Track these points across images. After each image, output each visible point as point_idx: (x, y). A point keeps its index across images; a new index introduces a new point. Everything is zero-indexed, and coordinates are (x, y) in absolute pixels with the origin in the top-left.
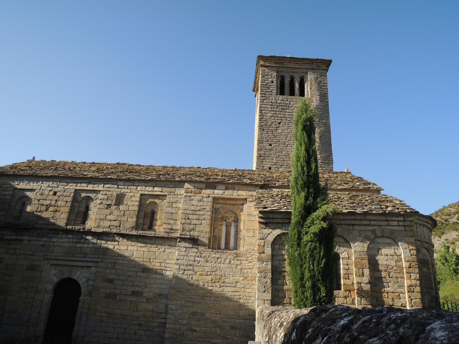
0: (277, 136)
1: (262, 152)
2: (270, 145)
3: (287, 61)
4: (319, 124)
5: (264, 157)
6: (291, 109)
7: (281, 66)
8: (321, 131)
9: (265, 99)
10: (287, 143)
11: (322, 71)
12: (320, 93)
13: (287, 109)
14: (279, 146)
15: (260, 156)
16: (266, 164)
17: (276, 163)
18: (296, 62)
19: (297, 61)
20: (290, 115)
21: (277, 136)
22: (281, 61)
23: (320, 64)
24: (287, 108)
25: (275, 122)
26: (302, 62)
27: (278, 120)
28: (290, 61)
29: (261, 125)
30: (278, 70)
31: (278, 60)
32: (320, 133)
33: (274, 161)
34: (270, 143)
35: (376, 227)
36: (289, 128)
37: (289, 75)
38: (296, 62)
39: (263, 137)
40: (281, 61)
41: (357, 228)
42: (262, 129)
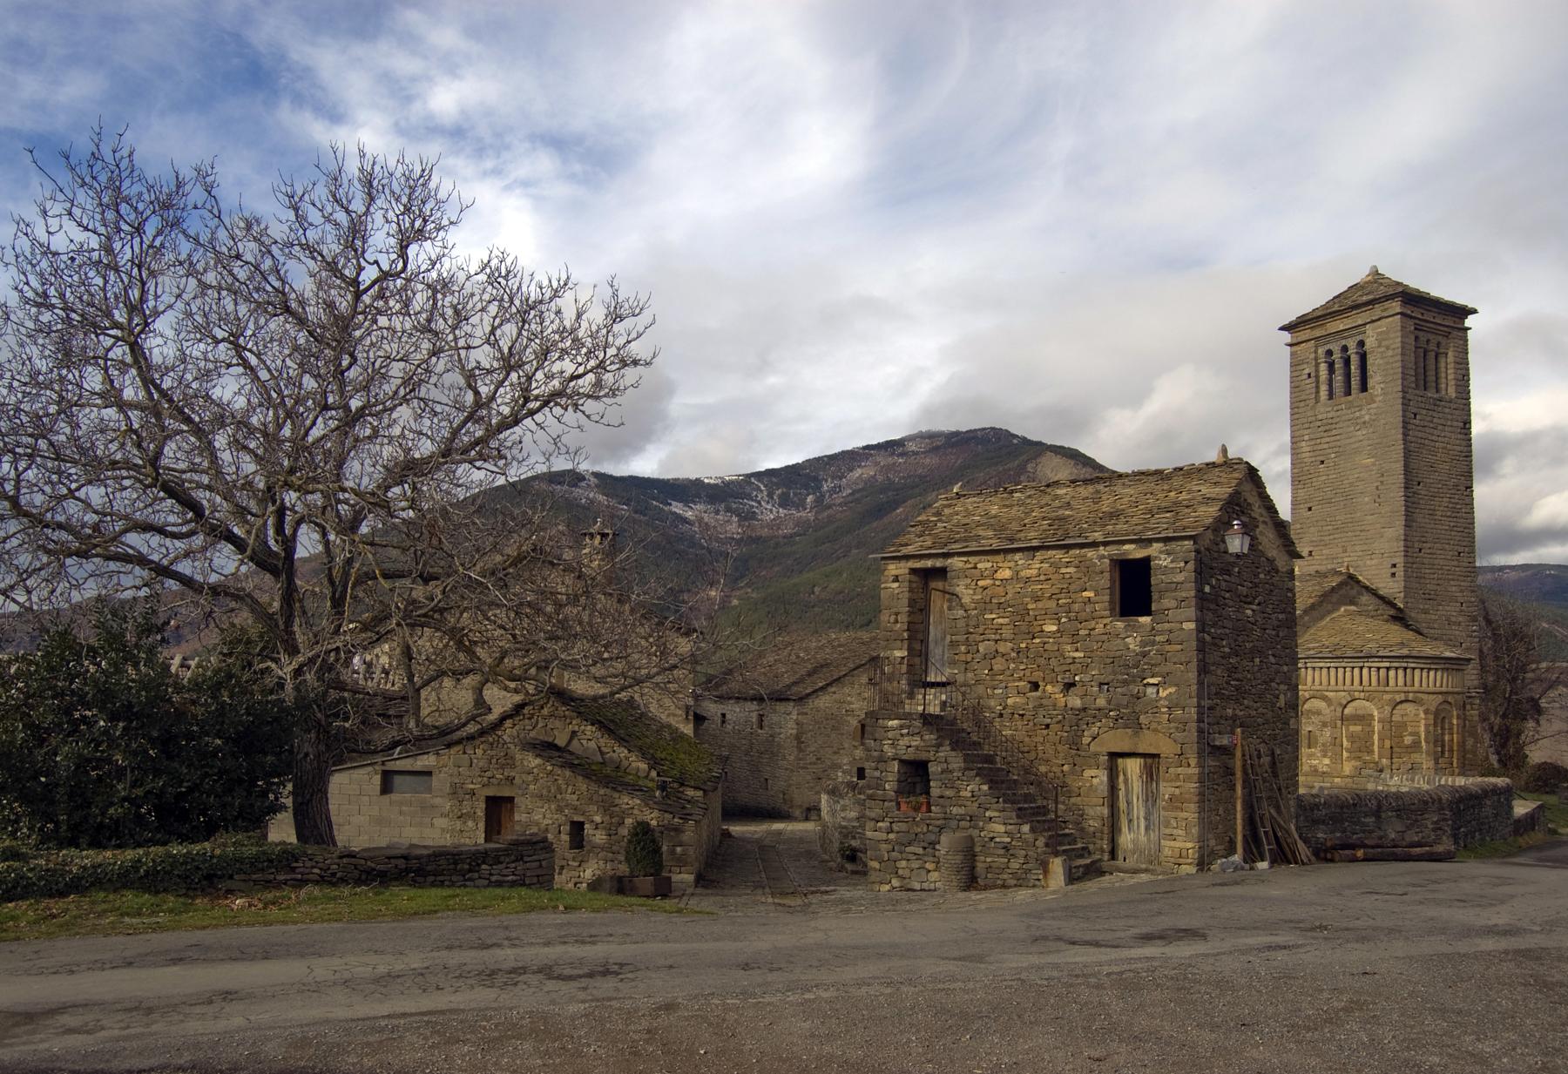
2: (1310, 509)
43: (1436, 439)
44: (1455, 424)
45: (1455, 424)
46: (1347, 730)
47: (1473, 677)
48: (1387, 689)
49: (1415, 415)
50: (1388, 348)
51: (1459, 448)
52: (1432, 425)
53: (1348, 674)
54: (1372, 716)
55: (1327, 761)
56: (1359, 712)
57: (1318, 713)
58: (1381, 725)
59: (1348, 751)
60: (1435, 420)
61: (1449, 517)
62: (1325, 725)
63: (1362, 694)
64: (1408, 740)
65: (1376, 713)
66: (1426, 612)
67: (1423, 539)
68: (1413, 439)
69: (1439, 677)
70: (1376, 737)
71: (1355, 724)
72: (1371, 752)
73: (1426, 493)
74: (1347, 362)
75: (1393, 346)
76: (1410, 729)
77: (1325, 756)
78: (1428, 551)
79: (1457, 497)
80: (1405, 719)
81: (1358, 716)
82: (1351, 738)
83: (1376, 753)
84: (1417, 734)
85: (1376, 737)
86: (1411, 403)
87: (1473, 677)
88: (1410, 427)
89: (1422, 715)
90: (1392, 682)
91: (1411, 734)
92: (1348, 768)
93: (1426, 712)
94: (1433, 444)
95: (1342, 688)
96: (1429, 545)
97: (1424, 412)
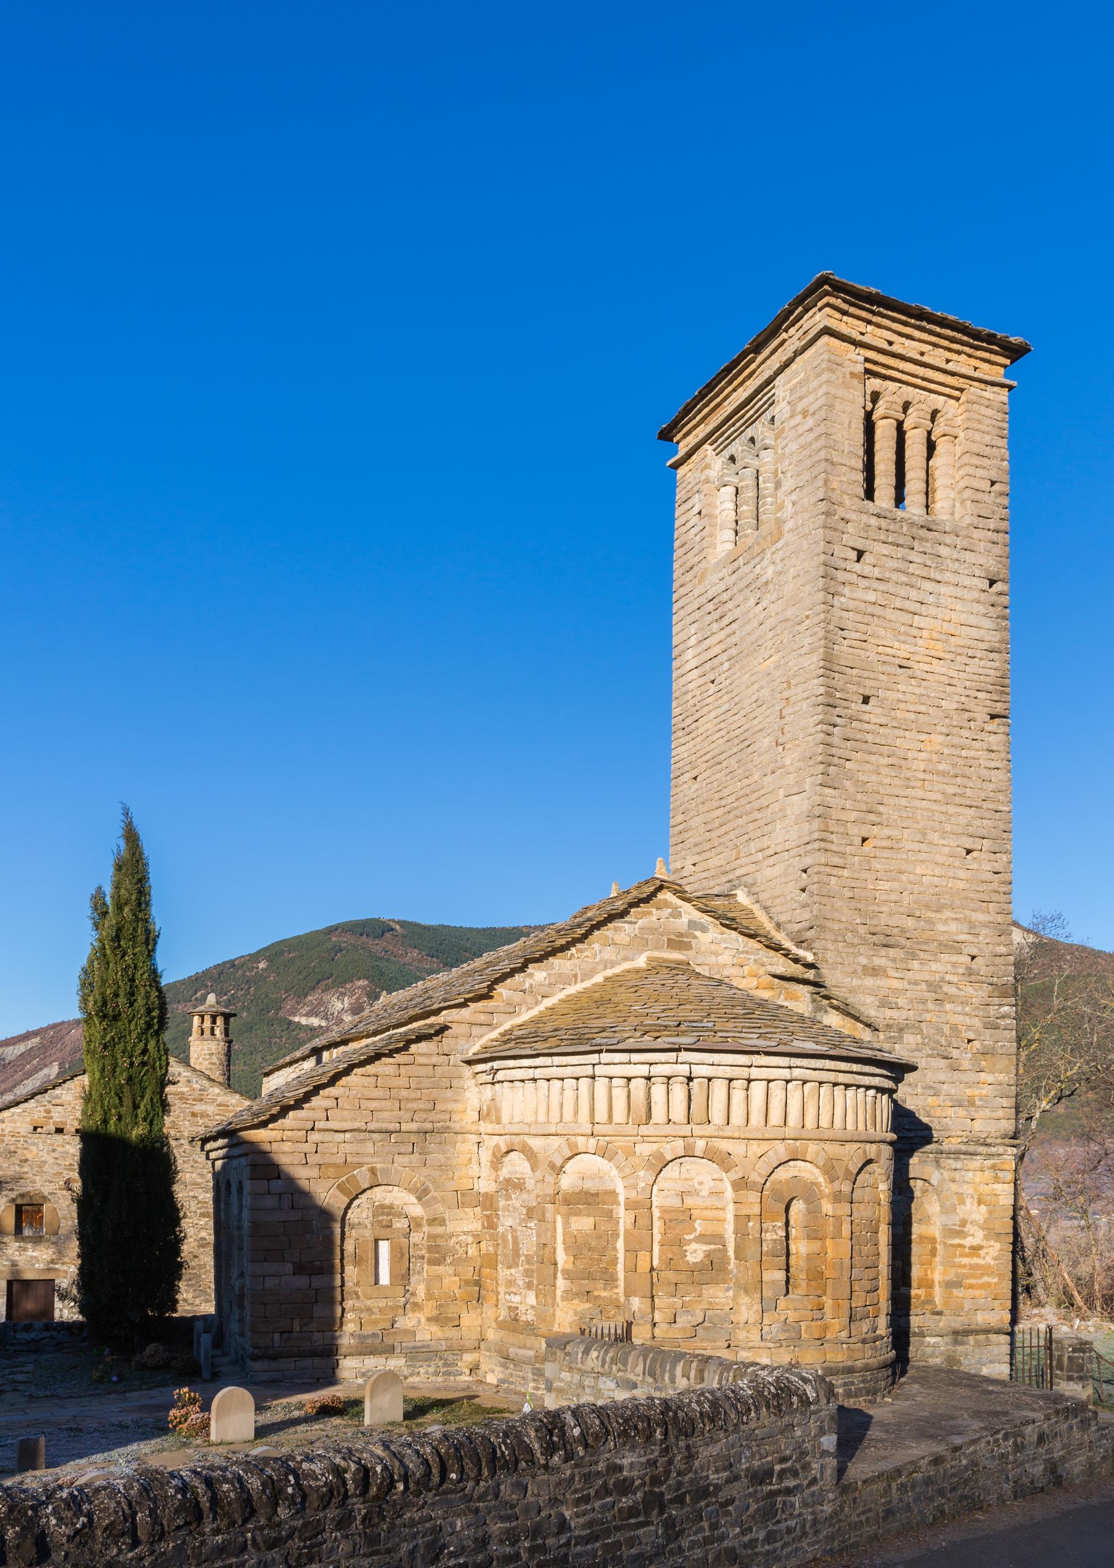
43: (916, 607)
44: (967, 581)
45: (967, 581)
46: (566, 1224)
47: (1000, 1113)
49: (860, 554)
50: (805, 413)
51: (975, 633)
52: (904, 578)
54: (613, 1194)
55: (532, 1299)
56: (589, 1185)
58: (631, 1215)
59: (568, 1275)
60: (912, 568)
61: (944, 774)
63: (592, 1142)
64: (696, 1253)
65: (620, 1189)
66: (875, 972)
67: (872, 817)
68: (852, 605)
70: (620, 1245)
72: (610, 1280)
73: (883, 721)
76: (699, 1226)
78: (885, 843)
79: (965, 733)
80: (689, 1201)
81: (587, 1193)
82: (575, 1246)
84: (718, 1238)
85: (620, 1245)
86: (850, 528)
87: (1000, 1113)
88: (841, 576)
89: (729, 1193)
91: (702, 1239)
93: (741, 1184)
94: (906, 618)
96: (887, 832)
97: (885, 549)
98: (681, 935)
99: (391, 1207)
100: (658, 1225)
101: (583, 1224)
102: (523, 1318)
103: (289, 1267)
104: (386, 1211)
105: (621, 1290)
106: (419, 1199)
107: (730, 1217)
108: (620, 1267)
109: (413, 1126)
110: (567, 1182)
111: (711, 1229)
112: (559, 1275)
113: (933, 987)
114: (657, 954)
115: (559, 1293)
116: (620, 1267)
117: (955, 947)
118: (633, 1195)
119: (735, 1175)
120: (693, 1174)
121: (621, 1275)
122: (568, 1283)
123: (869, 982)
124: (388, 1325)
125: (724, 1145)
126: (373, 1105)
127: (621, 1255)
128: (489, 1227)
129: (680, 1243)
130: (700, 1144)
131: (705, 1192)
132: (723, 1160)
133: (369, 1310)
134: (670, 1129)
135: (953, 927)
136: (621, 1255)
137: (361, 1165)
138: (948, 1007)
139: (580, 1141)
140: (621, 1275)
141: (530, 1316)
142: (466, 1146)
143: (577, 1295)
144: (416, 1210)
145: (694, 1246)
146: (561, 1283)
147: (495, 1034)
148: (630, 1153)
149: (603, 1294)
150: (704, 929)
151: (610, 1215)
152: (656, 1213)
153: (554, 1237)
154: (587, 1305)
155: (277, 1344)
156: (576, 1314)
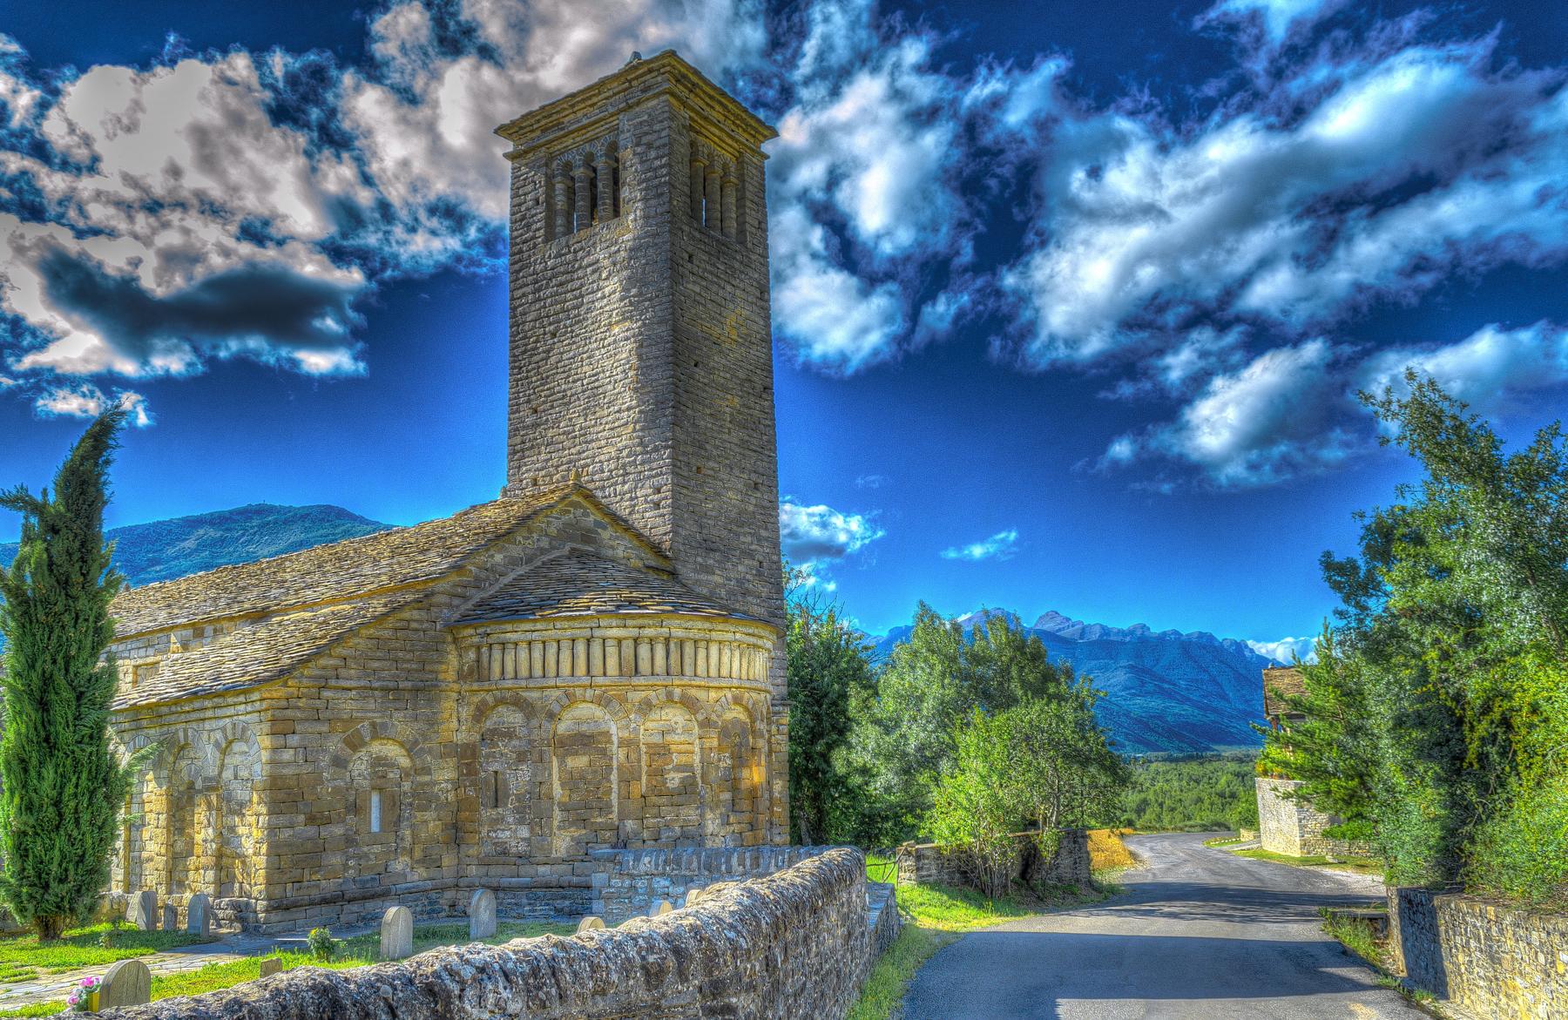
0: (548, 377)
1: (518, 439)
3: (565, 109)
4: (639, 302)
5: (523, 450)
6: (578, 279)
7: (551, 137)
8: (644, 324)
9: (520, 271)
10: (569, 393)
11: (654, 102)
12: (645, 189)
13: (568, 282)
14: (552, 407)
15: (515, 452)
16: (527, 471)
17: (547, 461)
18: (590, 102)
19: (589, 98)
20: (576, 298)
21: (548, 377)
22: (555, 117)
23: (648, 77)
24: (568, 277)
25: (545, 334)
26: (603, 96)
27: (550, 324)
28: (573, 106)
29: (514, 356)
30: (552, 150)
31: (545, 117)
32: (640, 334)
33: (543, 457)
34: (534, 404)
35: (228, 720)
36: (574, 343)
37: (580, 154)
38: (590, 102)
39: (518, 392)
40: (555, 117)
41: (207, 725)
42: (515, 368)
46: (562, 762)
47: (779, 681)
48: (636, 681)
49: (690, 257)
53: (565, 656)
54: (607, 734)
56: (584, 728)
57: (510, 734)
59: (565, 808)
62: (521, 758)
64: (674, 779)
65: (613, 730)
69: (726, 659)
70: (614, 777)
71: (576, 753)
72: (605, 809)
74: (593, 184)
75: (658, 143)
76: (676, 759)
77: (521, 822)
80: (668, 738)
82: (572, 781)
83: (615, 809)
85: (614, 777)
89: (696, 730)
90: (644, 666)
91: (678, 768)
92: (561, 843)
93: (706, 724)
95: (551, 683)
98: (589, 531)
99: (386, 758)
100: (644, 758)
101: (579, 762)
102: (514, 850)
103: (302, 818)
104: (379, 762)
105: (614, 816)
106: (409, 751)
107: (697, 749)
108: (614, 796)
109: (409, 684)
110: (563, 728)
111: (684, 759)
112: (555, 807)
113: (740, 582)
114: (575, 545)
115: (556, 823)
116: (614, 796)
117: (750, 554)
118: (626, 734)
119: (700, 717)
120: (670, 716)
121: (615, 802)
122: (565, 814)
123: (703, 577)
124: (382, 869)
125: (693, 692)
126: (376, 665)
127: (615, 786)
128: (468, 774)
129: (661, 772)
130: (678, 691)
131: (679, 731)
132: (690, 704)
133: (366, 855)
134: (652, 681)
135: (748, 539)
136: (615, 786)
137: (363, 719)
138: (750, 599)
139: (579, 692)
140: (615, 802)
141: (522, 847)
142: (448, 705)
143: (572, 824)
144: (405, 762)
145: (672, 775)
146: (558, 815)
147: (469, 605)
148: (623, 700)
149: (599, 820)
150: (605, 528)
151: (604, 753)
152: (644, 749)
153: (550, 775)
154: (584, 832)
155: (289, 894)
156: (573, 839)
